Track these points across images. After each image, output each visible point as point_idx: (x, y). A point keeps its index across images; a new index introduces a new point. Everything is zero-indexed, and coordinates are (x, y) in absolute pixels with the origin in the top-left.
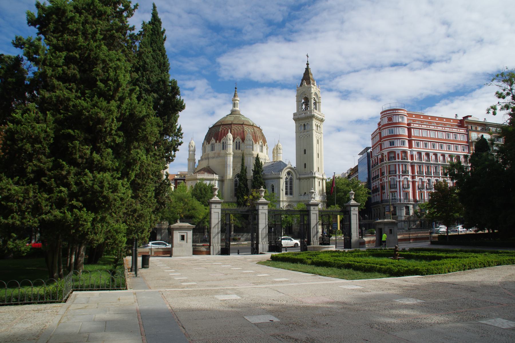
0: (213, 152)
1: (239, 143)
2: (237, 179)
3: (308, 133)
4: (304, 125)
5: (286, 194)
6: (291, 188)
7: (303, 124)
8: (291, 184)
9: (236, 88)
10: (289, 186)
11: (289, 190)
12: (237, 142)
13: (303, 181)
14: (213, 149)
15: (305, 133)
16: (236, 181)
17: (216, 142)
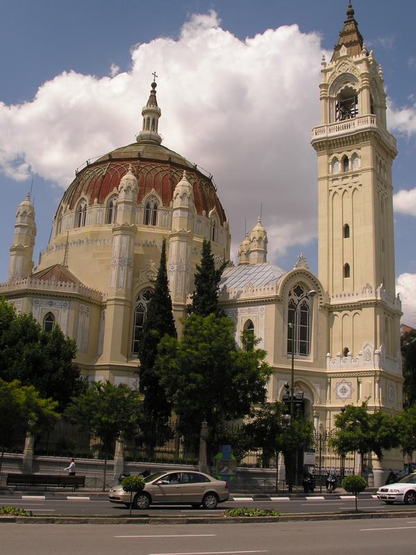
0: (82, 230)
1: (156, 207)
2: (145, 303)
3: (356, 179)
4: (345, 161)
5: (290, 349)
6: (304, 334)
7: (340, 156)
8: (305, 319)
9: (154, 85)
10: (298, 326)
11: (297, 341)
12: (148, 206)
13: (340, 314)
14: (80, 222)
15: (345, 181)
16: (140, 309)
17: (91, 203)
